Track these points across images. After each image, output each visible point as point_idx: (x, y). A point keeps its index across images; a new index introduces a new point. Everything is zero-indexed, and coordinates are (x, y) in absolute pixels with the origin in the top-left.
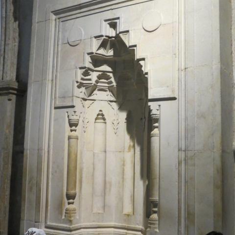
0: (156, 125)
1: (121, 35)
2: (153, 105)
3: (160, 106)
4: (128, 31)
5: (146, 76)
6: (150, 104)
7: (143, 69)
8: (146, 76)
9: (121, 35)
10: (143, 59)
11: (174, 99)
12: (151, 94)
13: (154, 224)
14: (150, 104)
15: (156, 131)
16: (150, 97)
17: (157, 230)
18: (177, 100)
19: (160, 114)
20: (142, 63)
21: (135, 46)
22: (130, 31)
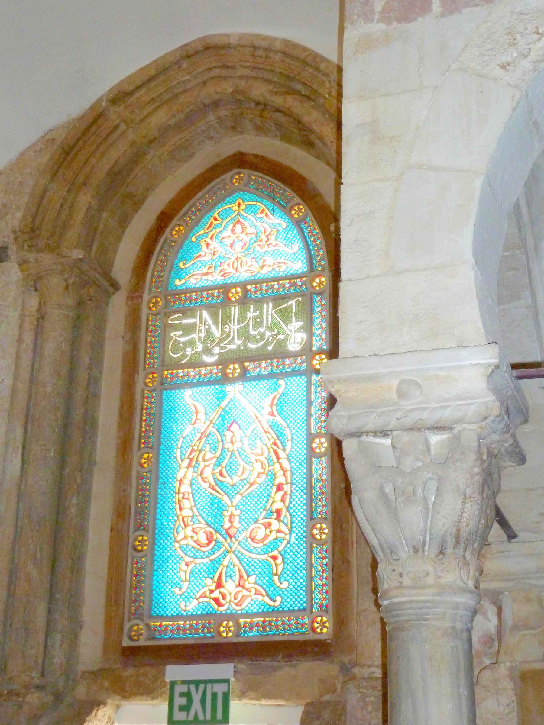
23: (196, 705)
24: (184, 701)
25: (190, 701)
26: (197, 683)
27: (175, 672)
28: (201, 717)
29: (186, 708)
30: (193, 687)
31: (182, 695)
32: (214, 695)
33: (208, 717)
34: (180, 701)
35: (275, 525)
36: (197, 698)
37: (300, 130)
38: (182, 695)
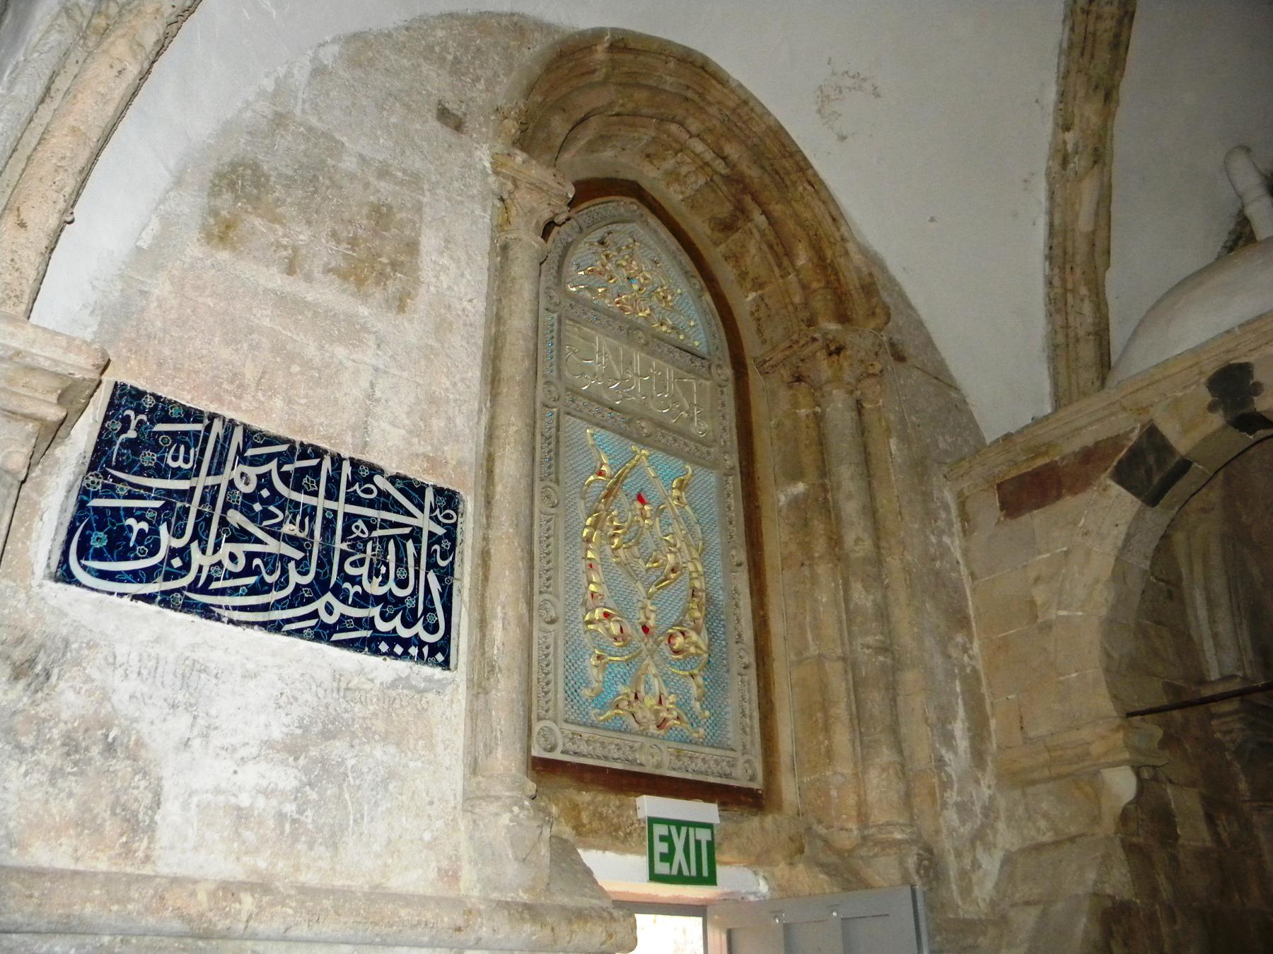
23: (679, 856)
24: (661, 847)
25: (672, 849)
26: (679, 824)
27: (649, 805)
28: (686, 872)
29: (668, 857)
30: (673, 829)
31: (662, 839)
32: (698, 843)
33: (694, 873)
34: (661, 847)
35: (694, 636)
36: (679, 844)
37: (736, 208)
38: (662, 839)
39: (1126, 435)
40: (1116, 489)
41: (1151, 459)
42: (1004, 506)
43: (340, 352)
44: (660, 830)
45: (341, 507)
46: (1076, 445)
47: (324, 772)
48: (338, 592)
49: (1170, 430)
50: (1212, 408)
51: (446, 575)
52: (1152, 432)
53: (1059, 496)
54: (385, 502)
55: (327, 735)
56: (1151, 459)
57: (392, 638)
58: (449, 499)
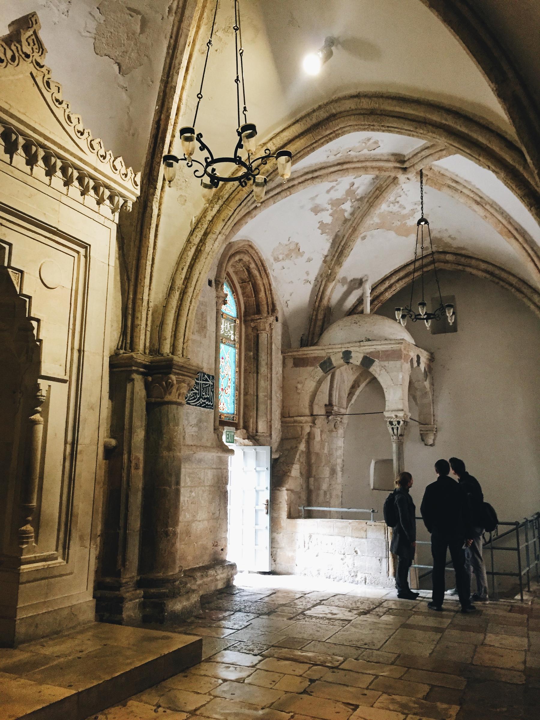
0: (39, 409)
1: (10, 270)
2: (43, 384)
3: (50, 386)
4: (22, 272)
5: (38, 343)
6: (40, 381)
7: (35, 332)
8: (38, 343)
9: (10, 270)
10: (38, 321)
11: (64, 381)
12: (45, 370)
13: (31, 537)
14: (40, 381)
15: (37, 417)
16: (43, 373)
17: (34, 544)
18: (67, 384)
19: (48, 397)
20: (35, 324)
21: (30, 298)
22: (25, 275)
29: (228, 438)
34: (228, 436)
39: (325, 357)
40: (319, 368)
41: (328, 364)
42: (294, 363)
43: (199, 349)
44: (228, 433)
45: (202, 382)
46: (313, 355)
47: (200, 428)
48: (202, 398)
49: (333, 359)
50: (342, 358)
51: (213, 392)
52: (329, 359)
53: (307, 366)
54: (206, 380)
55: (200, 422)
56: (328, 364)
57: (207, 405)
58: (213, 377)
